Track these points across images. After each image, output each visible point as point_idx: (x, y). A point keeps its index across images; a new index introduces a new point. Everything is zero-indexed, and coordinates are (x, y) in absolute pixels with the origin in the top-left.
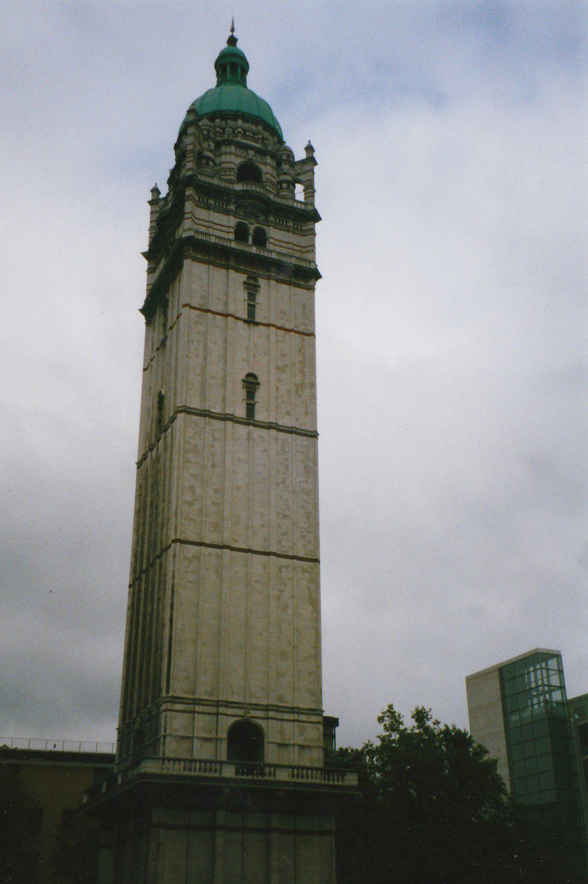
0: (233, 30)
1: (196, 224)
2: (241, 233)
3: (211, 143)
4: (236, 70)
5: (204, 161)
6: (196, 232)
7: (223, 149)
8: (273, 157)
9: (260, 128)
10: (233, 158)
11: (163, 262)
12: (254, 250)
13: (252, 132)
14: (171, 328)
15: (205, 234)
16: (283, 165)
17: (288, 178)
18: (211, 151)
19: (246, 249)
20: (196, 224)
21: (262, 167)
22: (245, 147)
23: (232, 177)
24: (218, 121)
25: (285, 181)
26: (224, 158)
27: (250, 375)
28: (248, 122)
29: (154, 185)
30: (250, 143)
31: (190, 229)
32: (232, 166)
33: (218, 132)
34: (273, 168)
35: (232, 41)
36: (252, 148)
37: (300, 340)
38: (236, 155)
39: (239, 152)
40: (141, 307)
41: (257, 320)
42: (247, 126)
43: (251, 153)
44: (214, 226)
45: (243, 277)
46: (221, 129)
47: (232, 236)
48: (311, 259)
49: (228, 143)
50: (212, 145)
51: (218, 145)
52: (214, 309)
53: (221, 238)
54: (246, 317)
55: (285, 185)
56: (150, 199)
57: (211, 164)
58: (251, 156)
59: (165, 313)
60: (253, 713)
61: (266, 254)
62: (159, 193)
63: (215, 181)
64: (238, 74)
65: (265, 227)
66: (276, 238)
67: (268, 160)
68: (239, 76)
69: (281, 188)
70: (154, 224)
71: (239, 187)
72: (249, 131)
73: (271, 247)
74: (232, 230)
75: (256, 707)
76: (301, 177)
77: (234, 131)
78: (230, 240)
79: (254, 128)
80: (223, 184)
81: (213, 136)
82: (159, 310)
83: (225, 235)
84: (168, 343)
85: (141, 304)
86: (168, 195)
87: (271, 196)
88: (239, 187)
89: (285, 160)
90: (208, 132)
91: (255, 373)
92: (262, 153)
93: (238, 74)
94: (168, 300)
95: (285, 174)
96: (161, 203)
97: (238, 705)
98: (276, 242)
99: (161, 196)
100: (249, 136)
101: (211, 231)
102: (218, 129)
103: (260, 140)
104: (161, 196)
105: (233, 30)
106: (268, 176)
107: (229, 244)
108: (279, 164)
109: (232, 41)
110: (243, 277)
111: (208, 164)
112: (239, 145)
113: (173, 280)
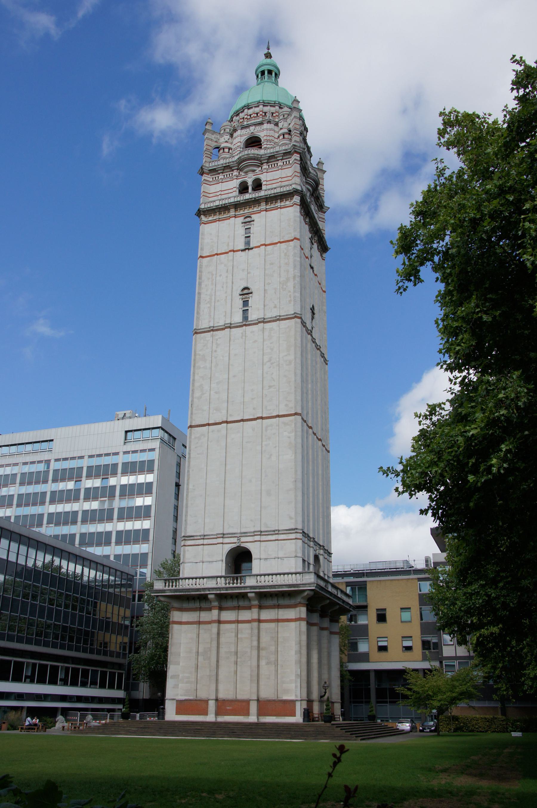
2: (243, 188)
4: (271, 74)
7: (235, 135)
27: (246, 288)
28: (252, 108)
37: (286, 246)
39: (244, 131)
49: (235, 130)
51: (232, 135)
58: (252, 131)
60: (243, 539)
75: (245, 534)
77: (272, 115)
91: (249, 286)
97: (232, 535)
100: (254, 117)
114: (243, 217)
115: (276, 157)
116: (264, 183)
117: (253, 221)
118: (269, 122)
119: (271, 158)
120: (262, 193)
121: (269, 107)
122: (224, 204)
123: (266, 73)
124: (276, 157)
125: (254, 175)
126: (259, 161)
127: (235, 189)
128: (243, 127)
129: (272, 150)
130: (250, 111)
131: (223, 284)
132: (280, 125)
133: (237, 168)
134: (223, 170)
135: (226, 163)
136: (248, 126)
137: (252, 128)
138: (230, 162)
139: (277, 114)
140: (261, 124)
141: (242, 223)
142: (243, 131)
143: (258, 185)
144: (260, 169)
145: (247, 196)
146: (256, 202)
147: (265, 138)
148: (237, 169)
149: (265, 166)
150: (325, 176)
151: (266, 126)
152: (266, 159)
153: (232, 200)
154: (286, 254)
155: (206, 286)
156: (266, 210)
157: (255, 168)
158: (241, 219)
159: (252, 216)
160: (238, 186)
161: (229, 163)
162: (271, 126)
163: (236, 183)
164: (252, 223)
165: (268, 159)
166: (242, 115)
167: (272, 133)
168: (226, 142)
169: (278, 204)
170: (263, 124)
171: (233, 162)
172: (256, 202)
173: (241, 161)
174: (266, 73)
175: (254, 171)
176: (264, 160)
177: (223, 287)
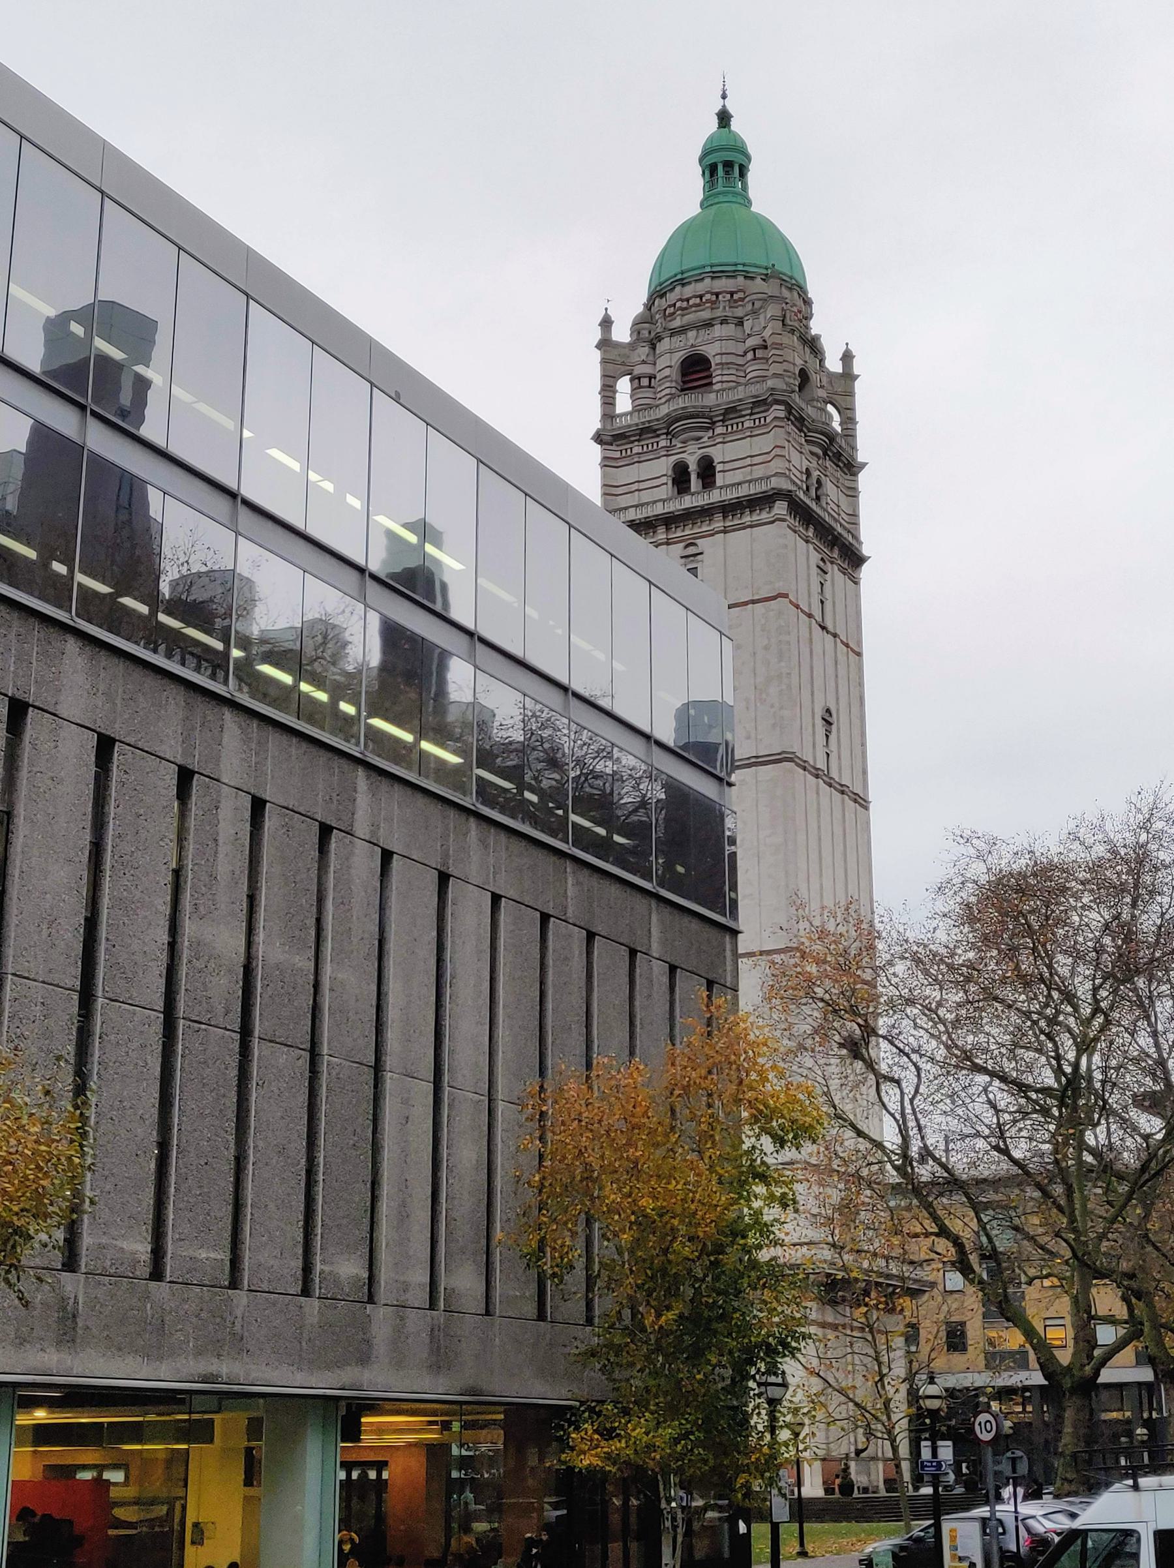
0: (724, 97)
35: (724, 118)
37: (763, 611)
39: (677, 342)
49: (659, 338)
58: (691, 341)
105: (724, 97)
109: (724, 118)
114: (682, 545)
116: (719, 468)
117: (701, 553)
118: (724, 321)
119: (731, 412)
120: (715, 496)
122: (645, 518)
123: (720, 168)
125: (699, 448)
126: (707, 421)
127: (664, 479)
128: (674, 333)
130: (688, 291)
132: (747, 325)
133: (665, 431)
135: (643, 423)
136: (683, 330)
137: (692, 334)
139: (741, 295)
140: (708, 324)
142: (674, 339)
143: (707, 471)
144: (710, 433)
145: (688, 502)
146: (706, 513)
147: (718, 359)
148: (667, 434)
149: (719, 430)
150: (857, 383)
151: (718, 330)
152: (721, 414)
153: (659, 509)
156: (725, 531)
158: (678, 549)
159: (697, 541)
160: (670, 473)
161: (649, 422)
162: (730, 330)
163: (663, 467)
164: (699, 557)
165: (724, 414)
167: (731, 347)
168: (644, 362)
169: (747, 519)
170: (713, 325)
171: (658, 420)
172: (706, 513)
173: (672, 420)
174: (720, 168)
176: (717, 416)
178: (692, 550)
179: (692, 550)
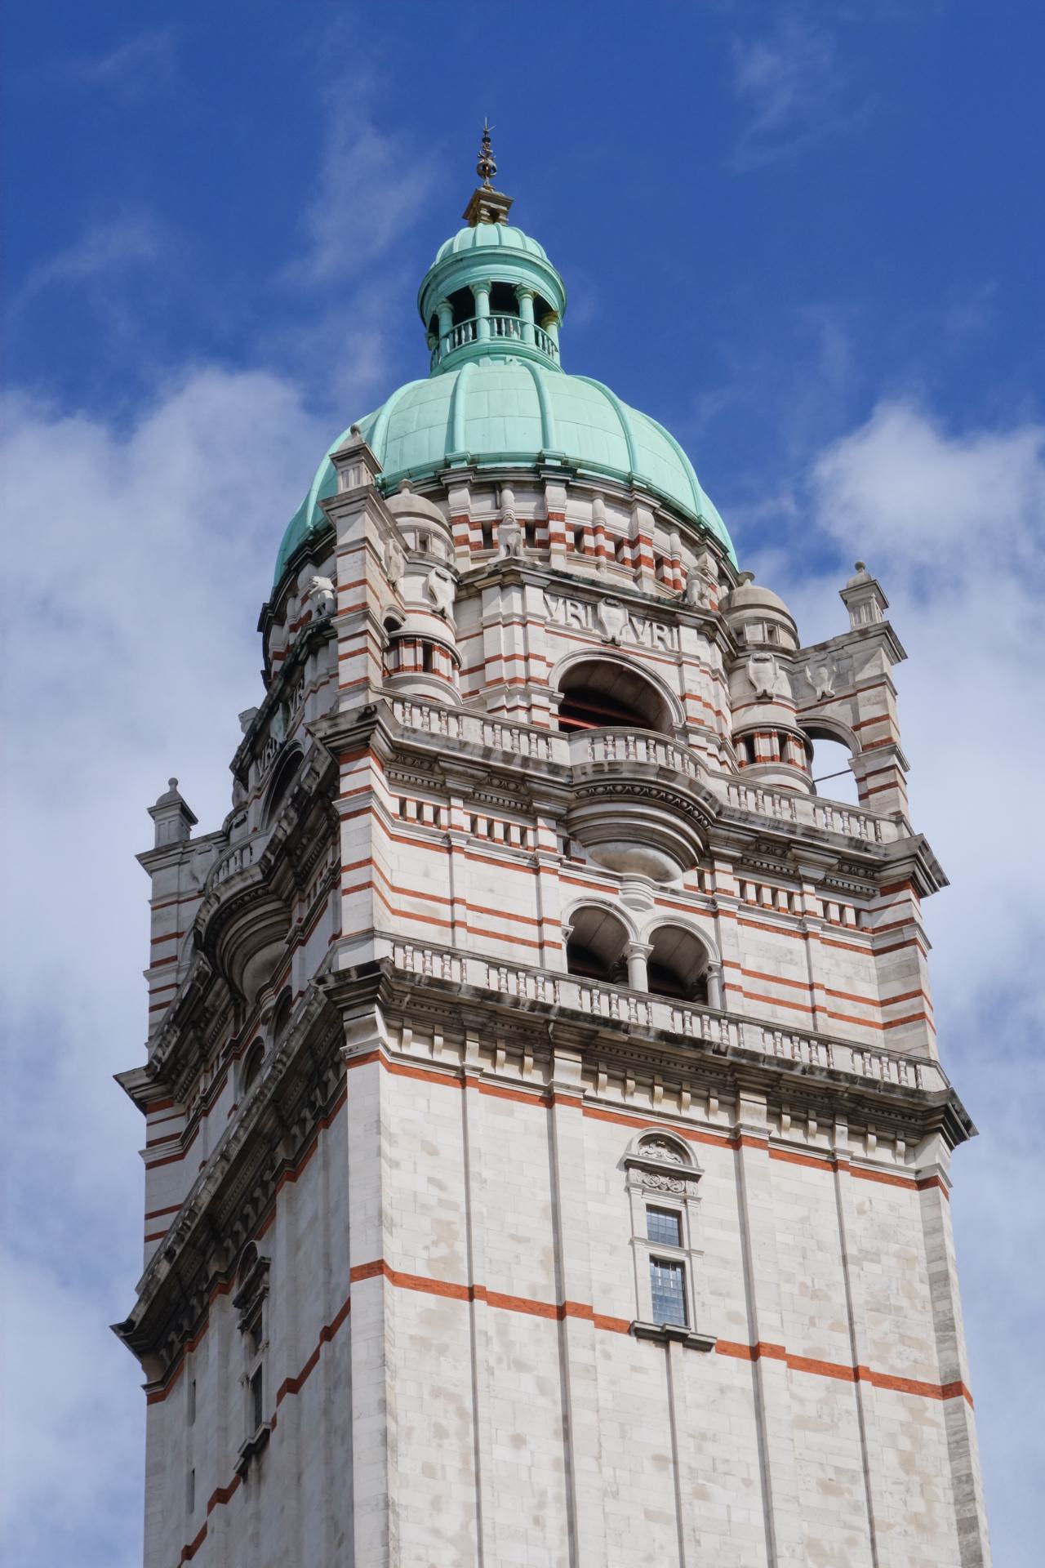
1: (394, 912)
3: (434, 581)
5: (410, 656)
6: (398, 942)
7: (499, 604)
8: (708, 630)
9: (644, 515)
10: (539, 641)
11: (228, 1096)
12: (663, 1016)
13: (609, 537)
14: (292, 1386)
15: (440, 951)
16: (751, 665)
17: (789, 719)
18: (441, 614)
19: (624, 1012)
20: (394, 912)
21: (668, 674)
22: (589, 594)
23: (539, 716)
24: (460, 497)
25: (766, 730)
26: (500, 641)
28: (588, 495)
29: (167, 789)
30: (606, 576)
31: (370, 934)
32: (538, 670)
33: (465, 540)
34: (715, 675)
36: (617, 598)
37: (903, 1415)
38: (554, 630)
39: (562, 610)
40: (122, 1319)
41: (703, 1325)
42: (580, 511)
43: (615, 618)
44: (473, 919)
45: (624, 1139)
46: (473, 526)
47: (558, 960)
48: (921, 1054)
49: (508, 577)
50: (446, 593)
52: (494, 1285)
53: (513, 969)
54: (648, 1318)
55: (764, 746)
56: (150, 846)
57: (441, 662)
58: (612, 632)
59: (252, 1327)
61: (714, 1033)
62: (189, 818)
63: (473, 732)
64: (523, 324)
65: (703, 925)
66: (749, 965)
67: (689, 639)
68: (530, 330)
69: (752, 758)
70: (183, 948)
71: (566, 753)
72: (595, 531)
73: (736, 1004)
74: (555, 934)
76: (837, 712)
78: (554, 978)
79: (617, 521)
80: (506, 742)
81: (442, 555)
82: (223, 1316)
83: (527, 956)
84: (277, 1453)
85: (126, 1304)
86: (235, 819)
87: (717, 787)
88: (566, 753)
89: (762, 647)
90: (424, 543)
92: (665, 614)
93: (523, 324)
94: (264, 1266)
95: (765, 698)
96: (201, 863)
98: (759, 986)
99: (196, 832)
100: (598, 551)
101: (464, 941)
102: (460, 530)
103: (649, 565)
104: (196, 832)
106: (693, 708)
107: (547, 995)
108: (735, 655)
110: (624, 1139)
111: (427, 666)
112: (562, 586)
113: (293, 1169)
114: (637, 1133)
115: (797, 860)
117: (695, 1178)
121: (676, 537)
124: (797, 860)
125: (659, 901)
129: (525, 747)
131: (541, 1505)
133: (560, 809)
134: (479, 784)
135: (508, 757)
138: (538, 763)
141: (628, 1164)
144: (691, 877)
154: (907, 1463)
155: (429, 1471)
157: (671, 865)
161: (526, 761)
162: (712, 655)
164: (690, 1185)
165: (744, 846)
166: (668, 542)
170: (677, 624)
171: (555, 769)
175: (663, 876)
176: (728, 841)
177: (537, 1521)
178: (666, 1158)
179: (663, 1157)
